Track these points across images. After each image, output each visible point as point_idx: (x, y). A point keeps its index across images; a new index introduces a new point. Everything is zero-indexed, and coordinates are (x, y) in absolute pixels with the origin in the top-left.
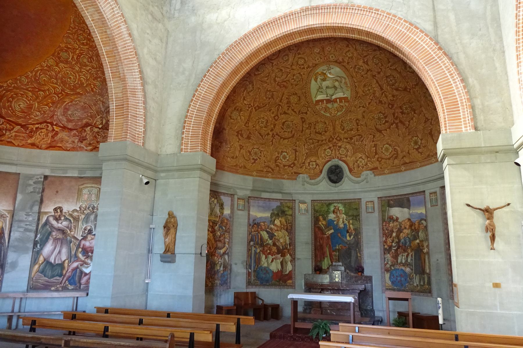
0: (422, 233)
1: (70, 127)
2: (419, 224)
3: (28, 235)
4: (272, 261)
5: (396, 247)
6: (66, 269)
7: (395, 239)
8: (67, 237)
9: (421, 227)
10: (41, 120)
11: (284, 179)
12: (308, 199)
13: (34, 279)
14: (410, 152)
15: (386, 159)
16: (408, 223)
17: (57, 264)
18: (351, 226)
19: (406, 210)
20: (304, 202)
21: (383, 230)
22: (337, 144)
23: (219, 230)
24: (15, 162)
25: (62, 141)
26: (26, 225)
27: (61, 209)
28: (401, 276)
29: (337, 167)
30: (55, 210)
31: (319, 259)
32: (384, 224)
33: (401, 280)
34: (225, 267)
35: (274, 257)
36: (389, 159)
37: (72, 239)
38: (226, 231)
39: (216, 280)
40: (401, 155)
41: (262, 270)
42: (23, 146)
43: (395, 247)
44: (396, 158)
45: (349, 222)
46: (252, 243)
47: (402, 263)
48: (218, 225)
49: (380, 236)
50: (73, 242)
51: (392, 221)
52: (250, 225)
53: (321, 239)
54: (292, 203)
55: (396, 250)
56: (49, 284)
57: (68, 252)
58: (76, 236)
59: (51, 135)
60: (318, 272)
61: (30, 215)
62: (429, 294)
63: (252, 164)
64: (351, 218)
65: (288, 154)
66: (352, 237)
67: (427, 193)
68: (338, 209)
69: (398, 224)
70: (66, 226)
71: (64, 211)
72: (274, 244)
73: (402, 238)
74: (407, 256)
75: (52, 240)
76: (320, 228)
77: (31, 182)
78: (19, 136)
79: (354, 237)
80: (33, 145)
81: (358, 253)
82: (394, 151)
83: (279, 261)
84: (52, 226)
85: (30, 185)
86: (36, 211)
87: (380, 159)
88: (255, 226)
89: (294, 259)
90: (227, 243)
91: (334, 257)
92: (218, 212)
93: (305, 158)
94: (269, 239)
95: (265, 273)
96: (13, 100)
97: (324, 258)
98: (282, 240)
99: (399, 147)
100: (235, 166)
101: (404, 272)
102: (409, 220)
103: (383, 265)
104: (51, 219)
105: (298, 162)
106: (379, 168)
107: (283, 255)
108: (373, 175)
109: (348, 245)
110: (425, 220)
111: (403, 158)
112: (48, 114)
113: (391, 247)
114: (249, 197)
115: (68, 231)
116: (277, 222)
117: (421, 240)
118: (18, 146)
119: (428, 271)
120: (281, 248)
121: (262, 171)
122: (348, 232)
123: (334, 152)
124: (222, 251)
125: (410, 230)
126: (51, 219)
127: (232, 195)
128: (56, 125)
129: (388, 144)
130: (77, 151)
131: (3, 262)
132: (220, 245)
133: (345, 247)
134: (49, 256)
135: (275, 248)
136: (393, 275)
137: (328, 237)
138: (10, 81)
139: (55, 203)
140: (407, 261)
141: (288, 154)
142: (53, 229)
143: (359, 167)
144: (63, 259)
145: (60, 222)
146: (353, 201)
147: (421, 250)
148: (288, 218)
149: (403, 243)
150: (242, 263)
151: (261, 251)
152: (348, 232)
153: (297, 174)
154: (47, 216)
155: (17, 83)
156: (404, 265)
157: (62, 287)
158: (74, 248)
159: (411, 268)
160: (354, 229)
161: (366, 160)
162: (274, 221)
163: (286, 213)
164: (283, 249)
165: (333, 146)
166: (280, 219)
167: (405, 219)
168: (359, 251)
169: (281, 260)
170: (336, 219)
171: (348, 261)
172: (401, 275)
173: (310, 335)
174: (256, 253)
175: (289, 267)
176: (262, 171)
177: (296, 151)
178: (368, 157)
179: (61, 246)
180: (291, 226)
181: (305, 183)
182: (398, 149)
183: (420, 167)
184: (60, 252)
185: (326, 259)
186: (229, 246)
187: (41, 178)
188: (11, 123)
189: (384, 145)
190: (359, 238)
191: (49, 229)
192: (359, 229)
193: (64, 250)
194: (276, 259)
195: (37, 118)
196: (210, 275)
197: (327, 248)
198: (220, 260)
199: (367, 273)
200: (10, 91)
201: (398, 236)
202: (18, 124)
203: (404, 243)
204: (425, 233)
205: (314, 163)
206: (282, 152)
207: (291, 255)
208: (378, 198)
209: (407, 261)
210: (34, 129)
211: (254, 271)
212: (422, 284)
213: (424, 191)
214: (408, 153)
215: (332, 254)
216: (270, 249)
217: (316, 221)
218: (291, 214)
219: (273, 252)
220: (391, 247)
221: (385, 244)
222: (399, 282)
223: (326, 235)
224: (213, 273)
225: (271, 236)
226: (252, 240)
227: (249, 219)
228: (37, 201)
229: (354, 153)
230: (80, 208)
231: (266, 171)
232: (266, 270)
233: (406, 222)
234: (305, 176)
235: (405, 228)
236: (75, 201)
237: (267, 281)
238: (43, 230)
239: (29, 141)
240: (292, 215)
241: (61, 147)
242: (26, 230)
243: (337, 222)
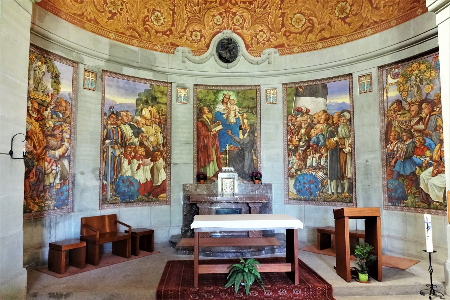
0: (343, 127)
2: (339, 117)
4: (138, 168)
5: (305, 147)
7: (303, 137)
9: (342, 121)
11: (156, 50)
12: (190, 82)
14: (332, 23)
15: (296, 34)
16: (323, 117)
18: (245, 121)
19: (321, 100)
20: (184, 87)
21: (288, 126)
22: (231, 9)
23: (52, 118)
28: (310, 182)
29: (230, 41)
31: (202, 164)
32: (289, 118)
33: (310, 188)
34: (64, 179)
35: (141, 162)
36: (301, 33)
38: (64, 121)
39: (46, 200)
40: (317, 28)
41: (123, 181)
43: (303, 146)
44: (311, 32)
45: (243, 116)
46: (108, 142)
47: (312, 167)
48: (49, 109)
49: (284, 134)
51: (300, 114)
52: (105, 114)
53: (206, 137)
54: (167, 87)
55: (305, 151)
60: (202, 181)
62: (350, 204)
63: (109, 19)
64: (246, 110)
65: (162, 16)
66: (246, 135)
67: (355, 77)
68: (229, 98)
69: (308, 118)
72: (142, 144)
73: (313, 135)
74: (320, 158)
76: (204, 124)
79: (249, 135)
81: (254, 156)
82: (309, 22)
83: (148, 168)
87: (287, 34)
88: (112, 115)
89: (170, 164)
90: (66, 140)
91: (222, 161)
92: (49, 86)
93: (186, 24)
94: (133, 137)
95: (128, 185)
97: (209, 163)
98: (152, 139)
99: (316, 17)
100: (79, 15)
101: (314, 177)
102: (325, 112)
103: (286, 169)
105: (176, 29)
106: (286, 45)
107: (154, 160)
108: (278, 54)
110: (349, 112)
111: (320, 31)
113: (297, 147)
114: (104, 71)
116: (146, 113)
117: (341, 136)
119: (349, 175)
120: (151, 149)
121: (124, 34)
122: (240, 128)
123: (225, 20)
124: (58, 153)
125: (325, 125)
127: (75, 63)
129: (300, 13)
132: (53, 142)
133: (237, 147)
135: (143, 149)
136: (299, 182)
137: (215, 135)
140: (319, 163)
141: (162, 16)
143: (258, 43)
146: (248, 88)
147: (341, 150)
148: (161, 107)
149: (314, 142)
150: (93, 171)
151: (121, 153)
152: (240, 128)
153: (175, 46)
156: (314, 169)
159: (325, 172)
160: (249, 125)
161: (268, 35)
162: (142, 110)
163: (158, 100)
164: (154, 151)
165: (226, 12)
166: (150, 108)
167: (318, 112)
168: (255, 153)
169: (151, 166)
170: (225, 112)
171: (241, 165)
172: (311, 181)
173: (228, 285)
174: (114, 156)
175: (162, 176)
176: (124, 34)
177: (174, 13)
178: (271, 31)
180: (166, 120)
181: (186, 59)
182: (315, 20)
183: (347, 42)
185: (211, 163)
186: (70, 144)
189: (295, 14)
190: (255, 136)
192: (255, 125)
194: (144, 164)
196: (35, 192)
198: (54, 168)
199: (264, 180)
201: (308, 133)
203: (316, 141)
204: (348, 128)
205: (199, 34)
206: (154, 10)
207: (164, 159)
208: (283, 84)
209: (319, 163)
211: (112, 183)
212: (340, 192)
213: (351, 74)
214: (330, 24)
215: (219, 157)
216: (136, 152)
217: (199, 113)
218: (165, 102)
219: (140, 155)
220: (297, 147)
221: (289, 143)
222: (307, 190)
223: (212, 132)
224: (41, 188)
225: (137, 132)
226: (108, 137)
227: (103, 105)
229: (253, 24)
231: (131, 36)
232: (130, 181)
233: (320, 114)
234: (187, 49)
235: (319, 123)
237: (131, 197)
240: (166, 104)
243: (227, 116)
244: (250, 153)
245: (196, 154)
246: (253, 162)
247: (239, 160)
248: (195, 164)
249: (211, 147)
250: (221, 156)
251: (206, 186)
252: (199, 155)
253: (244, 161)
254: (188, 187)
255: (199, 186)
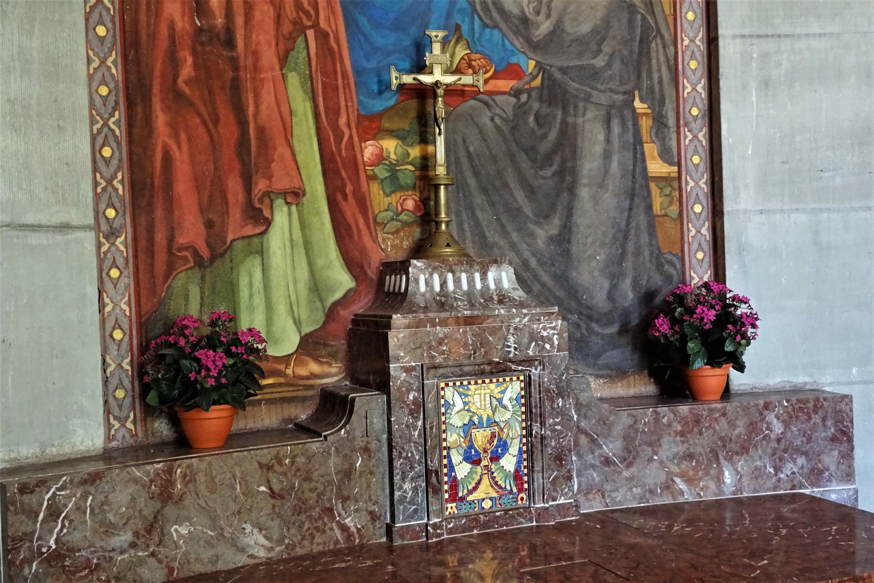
81: (651, 149)
109: (535, 46)
133: (513, 71)
168: (660, 122)
171: (542, 234)
197: (294, 80)
215: (354, 163)
244: (616, 128)
245: (116, 123)
246: (649, 207)
247: (531, 192)
248: (112, 235)
249: (269, 56)
250: (369, 150)
251: (267, 468)
252: (148, 119)
253: (572, 191)
254: (54, 513)
255: (189, 478)
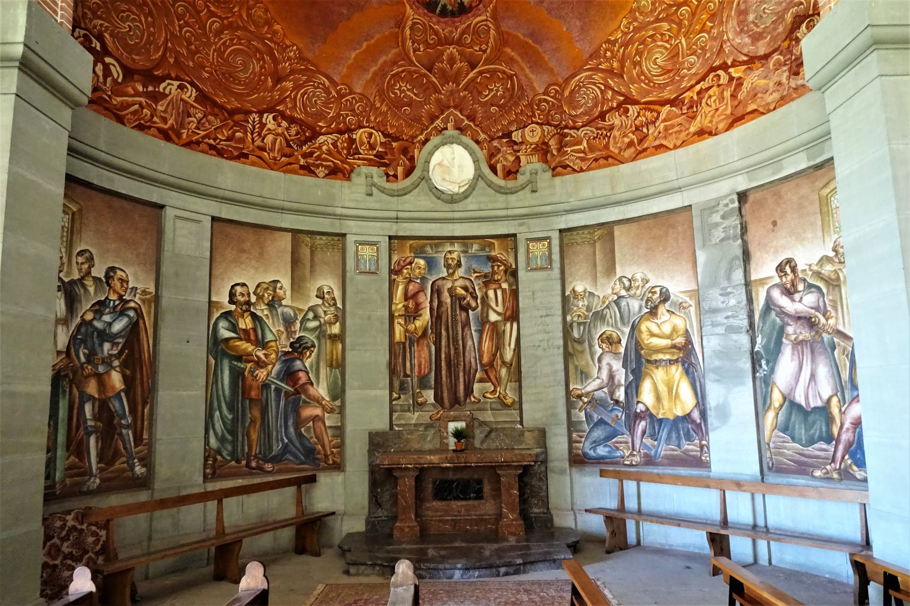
1: (762, 51)
3: (736, 341)
6: (839, 424)
8: (820, 335)
10: (702, 71)
13: (772, 445)
17: (815, 408)
24: (675, 184)
25: (756, 95)
26: (727, 318)
27: (793, 264)
30: (780, 269)
37: (835, 340)
42: (684, 144)
50: (839, 345)
56: (803, 459)
57: (833, 373)
58: (841, 328)
59: (729, 94)
61: (730, 293)
70: (812, 305)
71: (800, 267)
75: (790, 347)
77: (716, 218)
78: (673, 126)
80: (702, 133)
84: (782, 313)
85: (717, 225)
86: (738, 282)
96: (640, 57)
104: (776, 294)
112: (711, 48)
115: (821, 317)
118: (676, 147)
126: (776, 294)
128: (733, 66)
130: (793, 100)
131: (703, 405)
134: (793, 390)
138: (625, 22)
139: (776, 252)
142: (786, 319)
144: (825, 397)
145: (797, 296)
154: (766, 287)
155: (636, 19)
157: (839, 471)
158: (845, 365)
179: (813, 361)
184: (813, 376)
187: (732, 201)
188: (652, 107)
191: (778, 319)
193: (823, 371)
195: (693, 71)
200: (631, 42)
202: (663, 103)
210: (695, 98)
228: (736, 257)
230: (835, 250)
236: (820, 234)
238: (764, 323)
239: (692, 129)
241: (755, 110)
242: (731, 329)
